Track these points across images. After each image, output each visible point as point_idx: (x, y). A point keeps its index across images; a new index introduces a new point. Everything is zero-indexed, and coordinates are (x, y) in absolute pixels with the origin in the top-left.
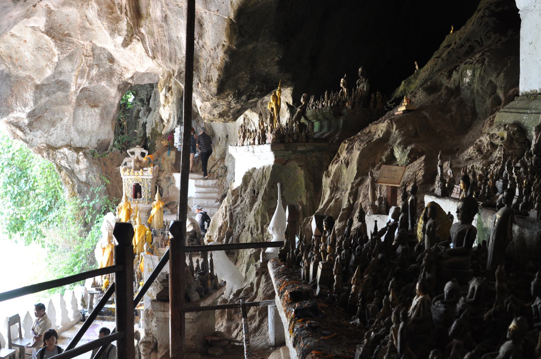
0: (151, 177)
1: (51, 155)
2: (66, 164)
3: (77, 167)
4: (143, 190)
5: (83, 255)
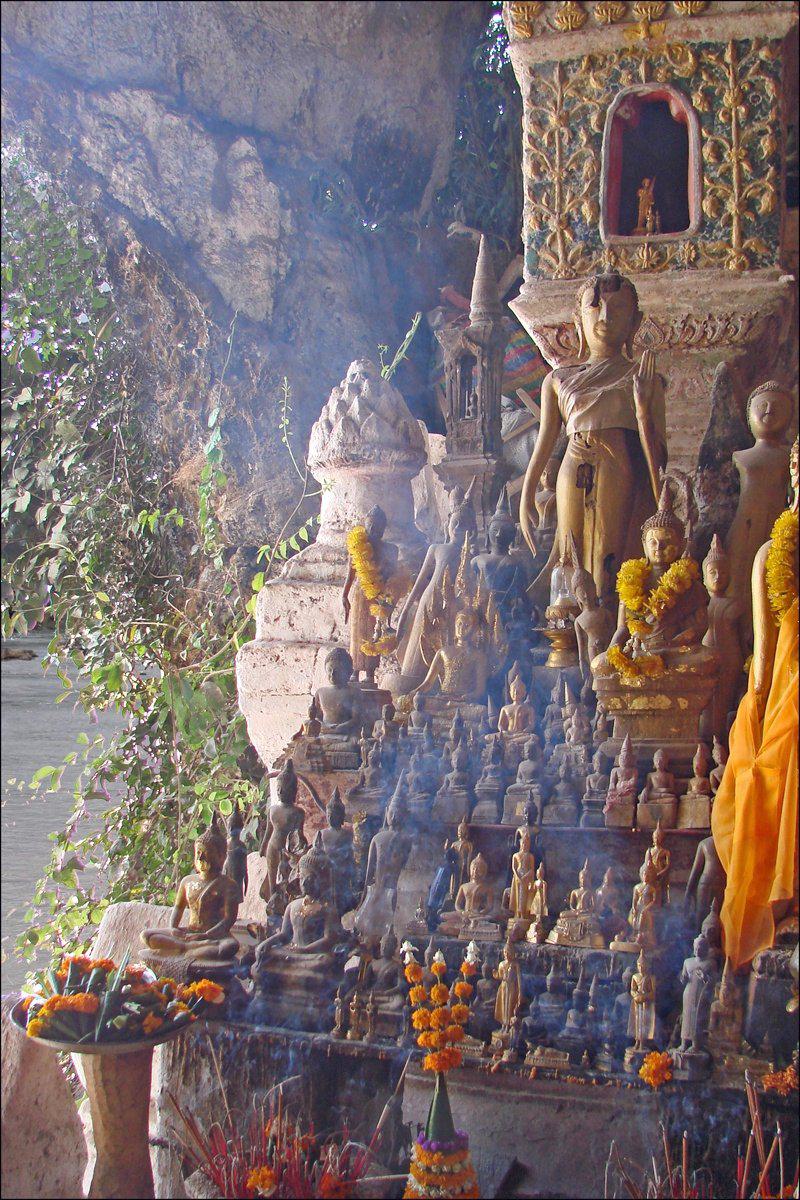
2: (143, 195)
3: (218, 231)
4: (697, 152)
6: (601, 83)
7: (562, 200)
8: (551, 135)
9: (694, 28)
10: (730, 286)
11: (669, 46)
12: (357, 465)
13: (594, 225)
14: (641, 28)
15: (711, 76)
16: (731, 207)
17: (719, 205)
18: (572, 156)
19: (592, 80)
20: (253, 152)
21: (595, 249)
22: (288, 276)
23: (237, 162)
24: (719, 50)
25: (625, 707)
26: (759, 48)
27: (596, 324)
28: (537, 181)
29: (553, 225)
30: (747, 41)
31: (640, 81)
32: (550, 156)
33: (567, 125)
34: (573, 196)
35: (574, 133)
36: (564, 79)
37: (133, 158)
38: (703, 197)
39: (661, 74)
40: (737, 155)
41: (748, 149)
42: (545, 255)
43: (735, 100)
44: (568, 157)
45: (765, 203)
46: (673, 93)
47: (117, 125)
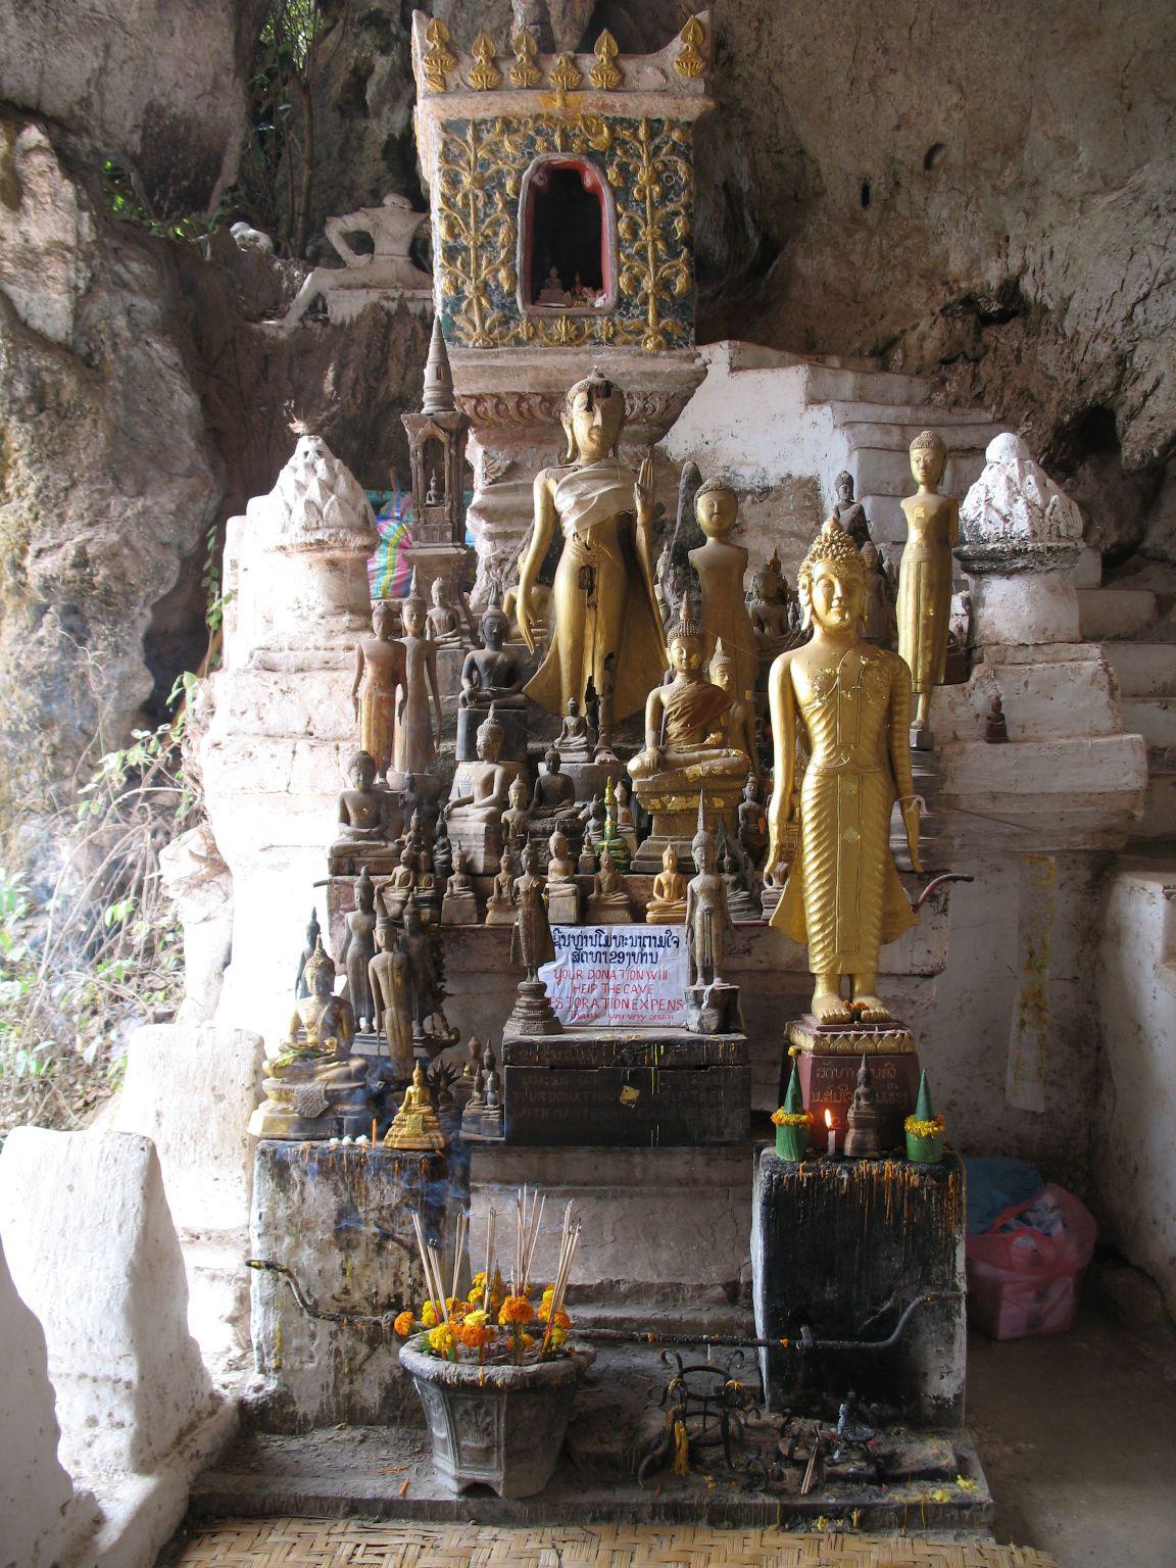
0: (694, 107)
4: (612, 225)
6: (516, 147)
7: (479, 266)
8: (465, 196)
9: (609, 102)
10: (649, 366)
11: (583, 117)
12: (322, 550)
13: (511, 293)
14: (558, 97)
15: (626, 152)
16: (648, 284)
17: (635, 282)
18: (488, 220)
19: (506, 143)
20: (45, 142)
21: (512, 318)
22: (89, 290)
23: (27, 153)
24: (632, 125)
25: (664, 807)
26: (671, 129)
27: (592, 428)
28: (451, 242)
29: (469, 289)
30: (659, 121)
31: (556, 150)
32: (465, 217)
33: (482, 188)
34: (490, 262)
35: (490, 197)
36: (478, 139)
38: (620, 272)
39: (576, 144)
40: (652, 234)
41: (663, 229)
42: (460, 320)
43: (650, 178)
44: (483, 221)
45: (680, 284)
46: (588, 165)
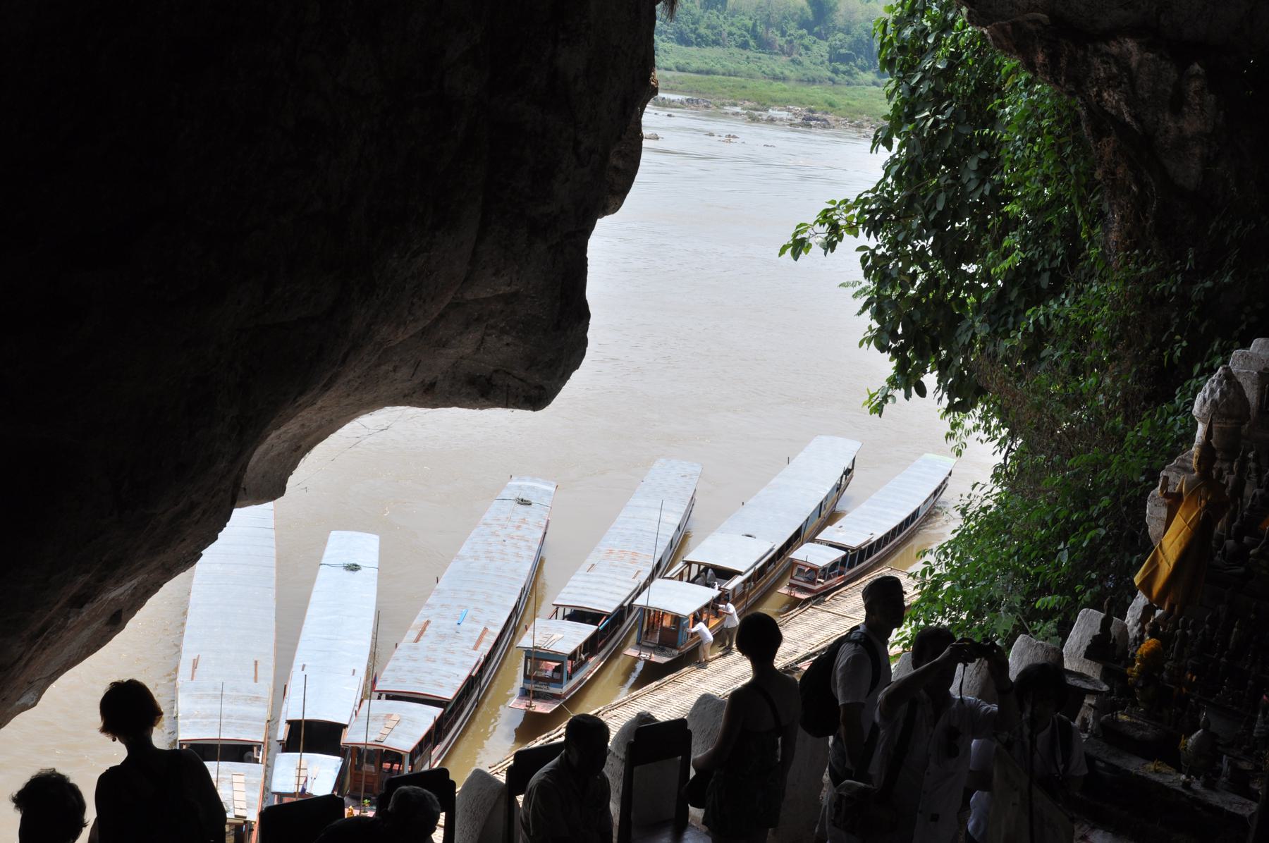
1: (1063, 62)
2: (1125, 109)
5: (1106, 501)
20: (1202, 71)
37: (1120, 84)
47: (1112, 61)
